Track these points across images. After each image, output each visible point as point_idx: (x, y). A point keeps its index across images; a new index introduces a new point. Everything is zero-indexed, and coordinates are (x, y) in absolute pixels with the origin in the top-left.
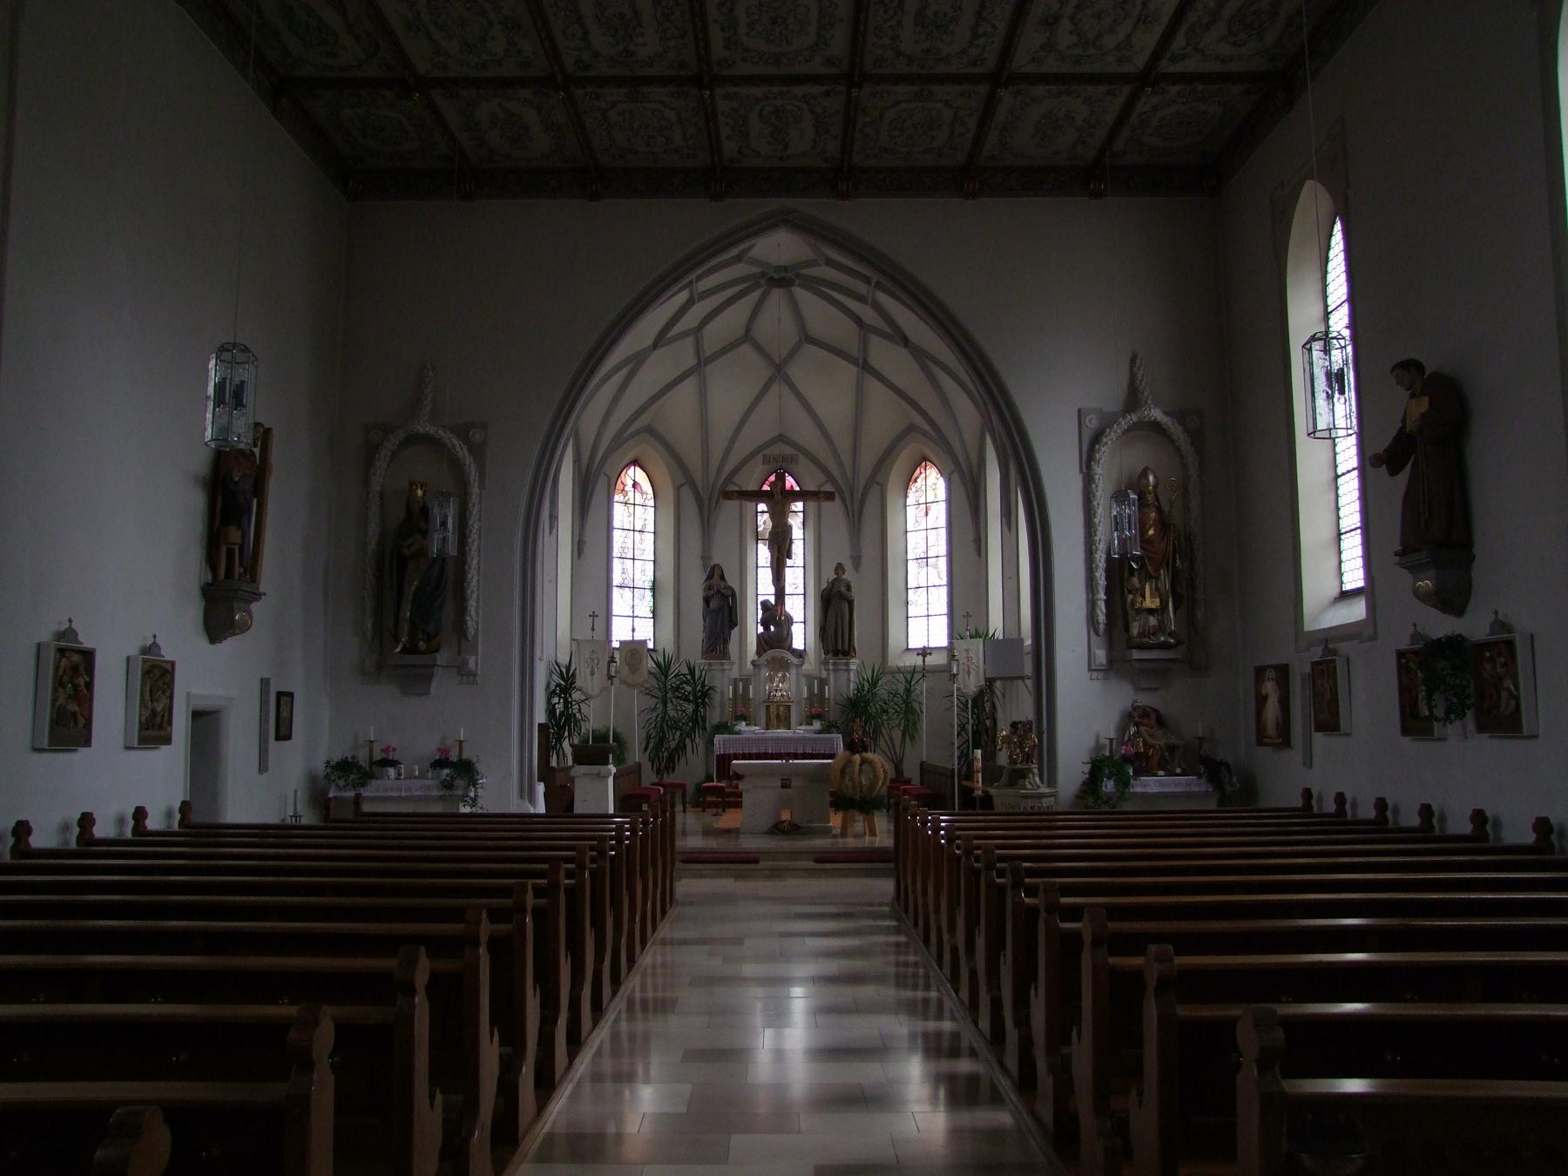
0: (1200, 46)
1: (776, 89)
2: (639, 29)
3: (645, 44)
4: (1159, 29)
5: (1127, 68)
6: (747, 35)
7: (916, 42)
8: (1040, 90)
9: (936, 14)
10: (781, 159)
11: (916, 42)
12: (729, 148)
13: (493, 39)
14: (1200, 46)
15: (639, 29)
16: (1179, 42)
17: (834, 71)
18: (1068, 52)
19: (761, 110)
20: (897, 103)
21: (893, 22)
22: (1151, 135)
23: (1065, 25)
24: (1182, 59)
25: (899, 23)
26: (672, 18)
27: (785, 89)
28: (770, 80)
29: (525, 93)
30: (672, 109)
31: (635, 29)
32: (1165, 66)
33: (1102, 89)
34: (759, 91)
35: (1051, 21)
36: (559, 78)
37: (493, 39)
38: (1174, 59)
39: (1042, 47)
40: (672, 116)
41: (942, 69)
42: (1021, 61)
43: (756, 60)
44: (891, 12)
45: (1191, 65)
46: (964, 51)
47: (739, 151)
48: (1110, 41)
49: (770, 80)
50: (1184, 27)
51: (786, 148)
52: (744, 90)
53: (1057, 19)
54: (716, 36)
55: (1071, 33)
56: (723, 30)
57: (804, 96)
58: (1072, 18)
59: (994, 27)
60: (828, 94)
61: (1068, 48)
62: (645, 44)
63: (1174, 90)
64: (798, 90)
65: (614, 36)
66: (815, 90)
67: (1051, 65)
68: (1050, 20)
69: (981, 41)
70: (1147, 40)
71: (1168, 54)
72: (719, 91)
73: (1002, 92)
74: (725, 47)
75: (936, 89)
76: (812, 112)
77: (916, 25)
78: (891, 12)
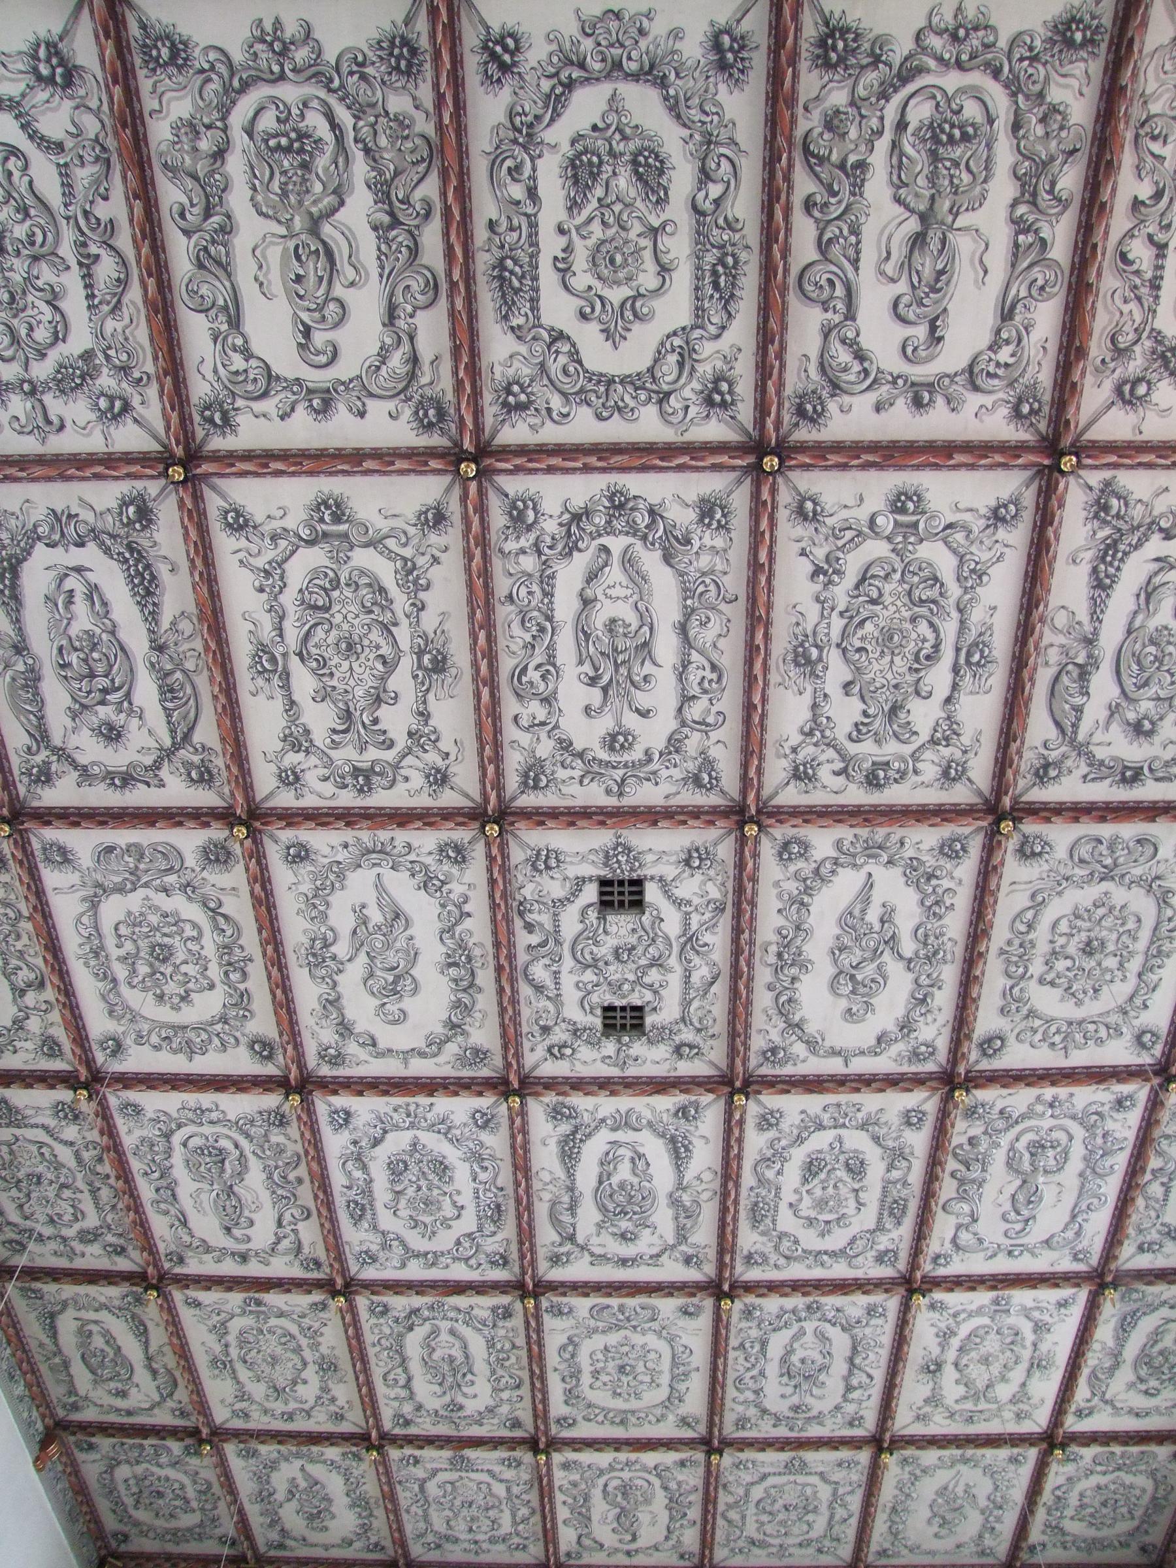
0: (1107, 1397)
1: (623, 1456)
2: (469, 1377)
3: (475, 1396)
4: (1056, 1376)
5: (1027, 1427)
6: (591, 1387)
7: (783, 1396)
8: (930, 1456)
9: (803, 1361)
10: (628, 1553)
11: (783, 1396)
12: (567, 1537)
13: (305, 1382)
14: (1107, 1397)
15: (469, 1377)
16: (1082, 1392)
17: (689, 1434)
18: (957, 1407)
19: (606, 1485)
20: (764, 1477)
21: (755, 1372)
22: (1072, 1518)
23: (949, 1374)
24: (1090, 1414)
25: (762, 1373)
26: (507, 1364)
27: (633, 1456)
28: (617, 1444)
29: (332, 1453)
30: (501, 1481)
31: (464, 1375)
32: (1072, 1424)
33: (1004, 1453)
34: (604, 1458)
35: (933, 1369)
36: (374, 1434)
37: (305, 1382)
38: (1080, 1414)
39: (927, 1401)
40: (500, 1490)
41: (814, 1431)
42: (904, 1422)
43: (600, 1418)
44: (752, 1360)
45: (1101, 1422)
46: (837, 1408)
47: (579, 1542)
48: (1004, 1392)
49: (617, 1444)
50: (1085, 1372)
51: (634, 1538)
52: (586, 1457)
53: (939, 1365)
54: (556, 1389)
55: (957, 1382)
56: (563, 1380)
57: (655, 1468)
58: (956, 1365)
59: (870, 1377)
60: (682, 1464)
61: (957, 1401)
62: (475, 1396)
63: (1088, 1453)
64: (650, 1458)
65: (440, 1384)
66: (669, 1457)
67: (939, 1425)
68: (932, 1367)
69: (855, 1395)
70: (1046, 1388)
71: (1073, 1408)
72: (557, 1458)
73: (886, 1458)
74: (566, 1403)
75: (810, 1456)
76: (666, 1488)
77: (782, 1375)
78: (752, 1360)
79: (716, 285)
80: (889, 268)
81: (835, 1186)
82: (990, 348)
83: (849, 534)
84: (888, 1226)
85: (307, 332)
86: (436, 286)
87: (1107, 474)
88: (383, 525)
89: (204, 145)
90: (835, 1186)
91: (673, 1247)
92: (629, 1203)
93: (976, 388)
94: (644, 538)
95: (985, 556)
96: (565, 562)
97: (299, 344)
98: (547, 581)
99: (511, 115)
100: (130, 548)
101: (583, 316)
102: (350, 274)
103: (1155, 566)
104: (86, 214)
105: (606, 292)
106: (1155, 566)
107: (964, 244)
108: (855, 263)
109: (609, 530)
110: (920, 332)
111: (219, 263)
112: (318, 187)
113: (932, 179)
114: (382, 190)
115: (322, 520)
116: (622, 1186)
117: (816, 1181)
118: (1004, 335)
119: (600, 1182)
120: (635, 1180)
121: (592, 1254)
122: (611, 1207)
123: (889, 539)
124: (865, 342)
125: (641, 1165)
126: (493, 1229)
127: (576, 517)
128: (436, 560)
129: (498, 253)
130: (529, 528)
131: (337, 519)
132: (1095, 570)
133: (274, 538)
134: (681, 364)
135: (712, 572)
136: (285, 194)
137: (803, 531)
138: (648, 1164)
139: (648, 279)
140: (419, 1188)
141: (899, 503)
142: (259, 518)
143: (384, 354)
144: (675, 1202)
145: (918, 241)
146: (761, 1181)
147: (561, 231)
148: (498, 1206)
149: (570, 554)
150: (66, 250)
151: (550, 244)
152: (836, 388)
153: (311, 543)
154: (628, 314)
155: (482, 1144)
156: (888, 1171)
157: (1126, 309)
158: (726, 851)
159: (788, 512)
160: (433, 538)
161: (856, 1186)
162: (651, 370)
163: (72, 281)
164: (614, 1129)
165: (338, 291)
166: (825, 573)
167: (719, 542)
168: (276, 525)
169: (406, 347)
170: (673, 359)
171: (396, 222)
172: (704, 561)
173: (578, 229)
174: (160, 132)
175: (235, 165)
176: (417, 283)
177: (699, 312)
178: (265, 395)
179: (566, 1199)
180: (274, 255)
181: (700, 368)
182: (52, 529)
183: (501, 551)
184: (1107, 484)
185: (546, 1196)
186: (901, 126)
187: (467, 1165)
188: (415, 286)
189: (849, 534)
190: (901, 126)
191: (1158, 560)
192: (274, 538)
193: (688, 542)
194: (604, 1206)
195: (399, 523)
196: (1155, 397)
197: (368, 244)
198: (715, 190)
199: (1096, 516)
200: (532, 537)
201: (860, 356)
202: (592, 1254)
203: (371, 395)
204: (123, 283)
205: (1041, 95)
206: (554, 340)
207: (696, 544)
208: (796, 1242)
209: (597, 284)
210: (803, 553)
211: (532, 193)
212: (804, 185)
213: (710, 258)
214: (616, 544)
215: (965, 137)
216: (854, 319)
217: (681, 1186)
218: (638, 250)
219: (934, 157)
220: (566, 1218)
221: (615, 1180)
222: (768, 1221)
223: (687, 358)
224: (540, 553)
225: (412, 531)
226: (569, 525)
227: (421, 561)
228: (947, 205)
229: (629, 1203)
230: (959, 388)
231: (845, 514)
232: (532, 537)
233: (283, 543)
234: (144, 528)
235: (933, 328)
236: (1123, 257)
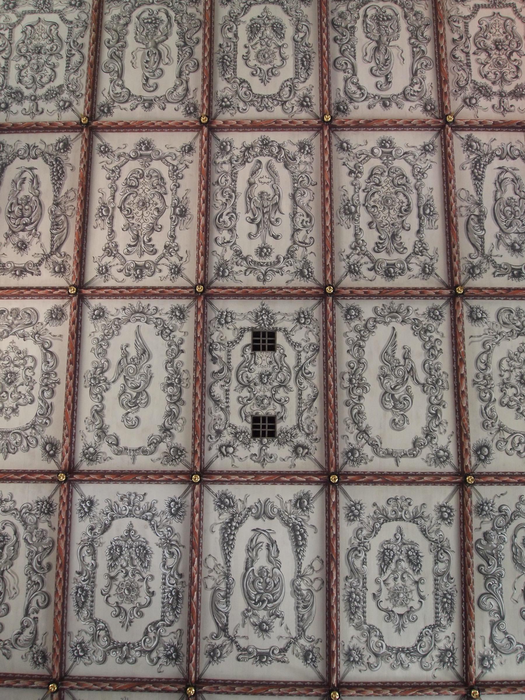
79: (303, 65)
80: (367, 58)
81: (403, 578)
82: (410, 85)
83: (363, 157)
84: (444, 622)
85: (147, 79)
86: (198, 65)
87: (468, 133)
88: (166, 151)
89: (122, 22)
90: (403, 578)
91: (296, 639)
92: (266, 591)
93: (407, 100)
94: (276, 157)
95: (423, 166)
96: (242, 167)
97: (144, 84)
98: (234, 175)
99: (230, 13)
100: (56, 160)
101: (253, 74)
102: (167, 60)
103: (499, 171)
104: (74, 41)
105: (262, 67)
106: (499, 171)
107: (394, 52)
108: (354, 57)
109: (261, 154)
110: (382, 80)
111: (118, 57)
112: (159, 34)
113: (379, 30)
114: (182, 35)
115: (141, 149)
116: (261, 570)
117: (389, 572)
118: (415, 81)
119: (247, 569)
120: (269, 567)
121: (239, 648)
122: (253, 593)
123: (380, 158)
124: (361, 83)
125: (273, 550)
126: (171, 618)
127: (248, 149)
128: (187, 166)
129: (222, 54)
130: (228, 153)
131: (147, 149)
132: (473, 172)
133: (119, 157)
134: (290, 91)
135: (305, 172)
136: (147, 35)
137: (343, 155)
138: (278, 551)
139: (278, 62)
140: (127, 574)
141: (383, 144)
142: (114, 149)
143: (175, 88)
144: (296, 591)
145: (377, 49)
146: (354, 571)
147: (246, 47)
148: (177, 593)
149: (244, 164)
150: (64, 53)
151: (241, 51)
152: (351, 100)
153: (134, 159)
154: (270, 74)
155: (172, 531)
156: (436, 563)
157: (460, 73)
158: (317, 314)
159: (336, 148)
160: (187, 157)
161: (417, 578)
162: (279, 93)
163: (62, 63)
164: (257, 518)
165: (161, 66)
166: (355, 173)
167: (308, 160)
168: (121, 151)
169: (184, 85)
170: (287, 89)
171: (186, 44)
172: (302, 167)
173: (252, 46)
174: (107, 19)
175: (131, 28)
176: (191, 64)
177: (297, 73)
178: (127, 101)
179: (223, 586)
180: (139, 54)
181: (298, 93)
182: (25, 152)
183: (215, 162)
184: (469, 137)
185: (210, 583)
186: (365, 16)
187: (161, 550)
188: (190, 65)
189: (363, 157)
190: (365, 16)
191: (499, 168)
192: (119, 157)
193: (295, 159)
194: (248, 593)
195: (173, 151)
196: (480, 104)
197: (175, 52)
198: (301, 35)
199: (468, 149)
200: (229, 156)
201: (360, 88)
202: (239, 648)
203: (169, 102)
204: (81, 63)
205: (412, 9)
206: (241, 83)
207: (298, 160)
208: (381, 637)
209: (259, 64)
210: (344, 164)
211: (236, 36)
212: (333, 34)
213: (301, 56)
214: (264, 160)
215: (388, 19)
216: (356, 75)
217: (300, 575)
218: (274, 53)
219: (378, 24)
220: (222, 607)
221: (256, 566)
222: (360, 613)
223: (292, 89)
224: (231, 163)
225: (178, 154)
226: (244, 152)
227: (180, 166)
228: (385, 39)
229: (266, 591)
230: (400, 100)
231: (360, 148)
232: (229, 156)
233: (122, 159)
234: (65, 151)
235: (387, 78)
236: (454, 56)
